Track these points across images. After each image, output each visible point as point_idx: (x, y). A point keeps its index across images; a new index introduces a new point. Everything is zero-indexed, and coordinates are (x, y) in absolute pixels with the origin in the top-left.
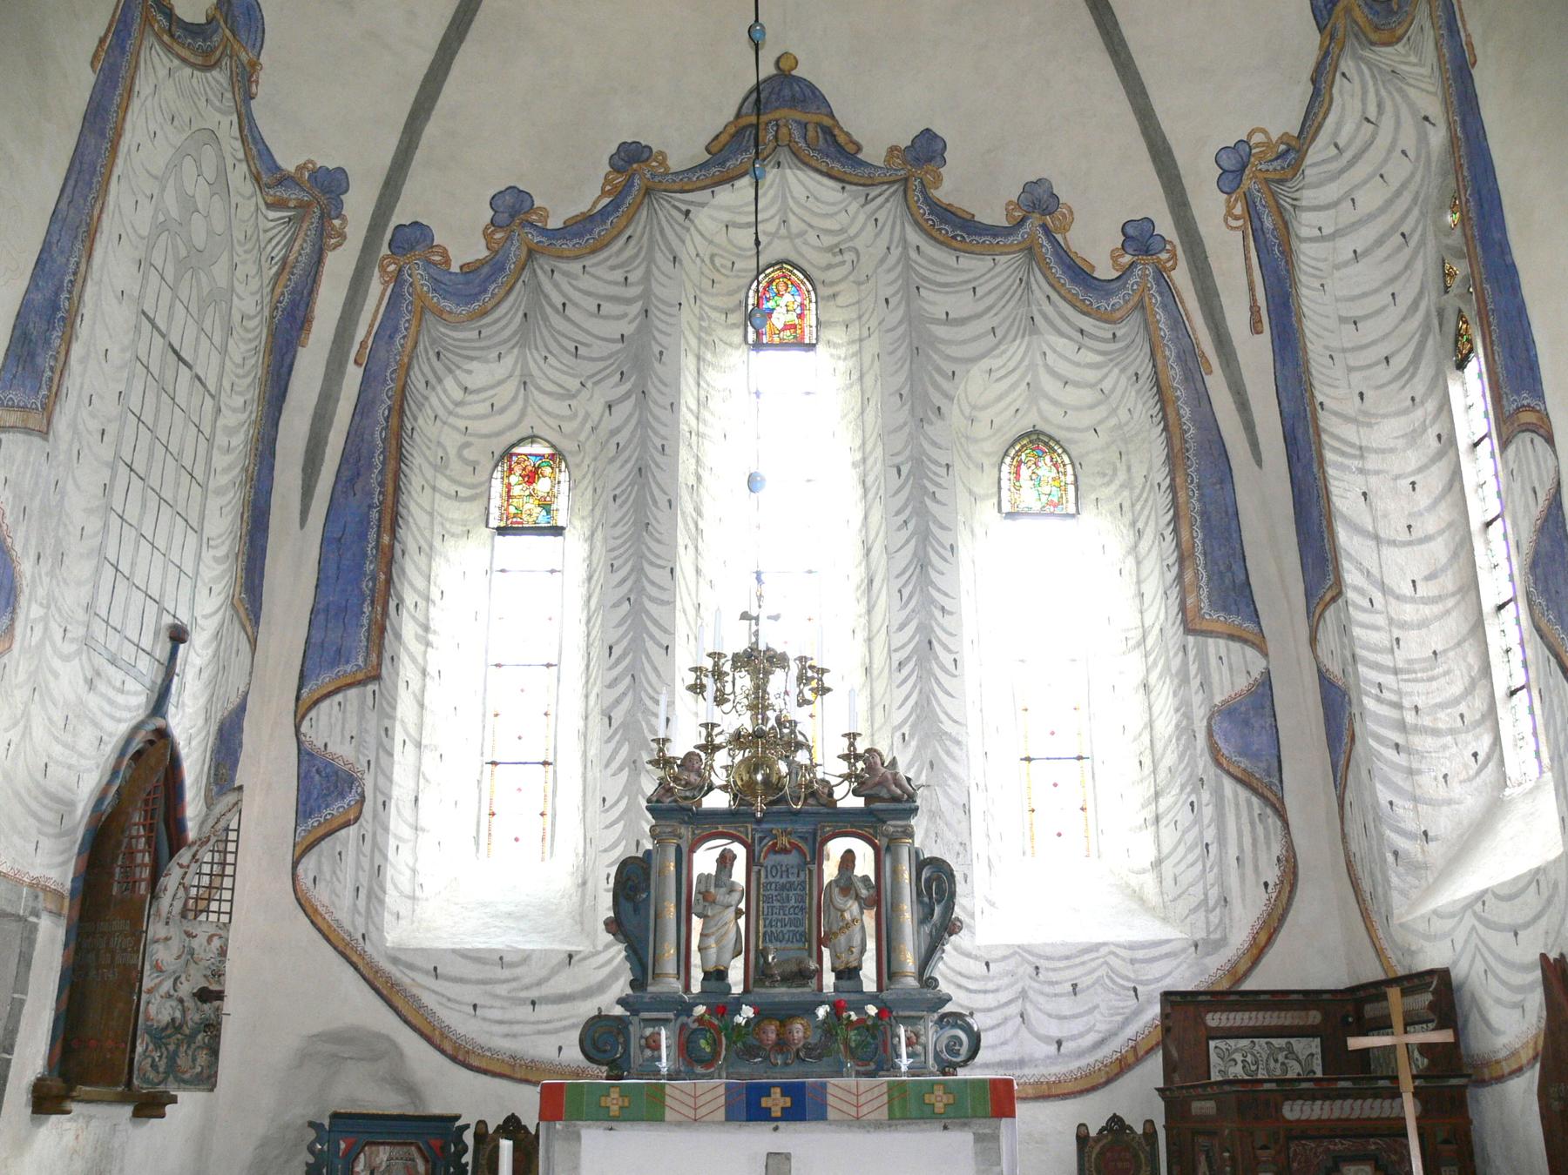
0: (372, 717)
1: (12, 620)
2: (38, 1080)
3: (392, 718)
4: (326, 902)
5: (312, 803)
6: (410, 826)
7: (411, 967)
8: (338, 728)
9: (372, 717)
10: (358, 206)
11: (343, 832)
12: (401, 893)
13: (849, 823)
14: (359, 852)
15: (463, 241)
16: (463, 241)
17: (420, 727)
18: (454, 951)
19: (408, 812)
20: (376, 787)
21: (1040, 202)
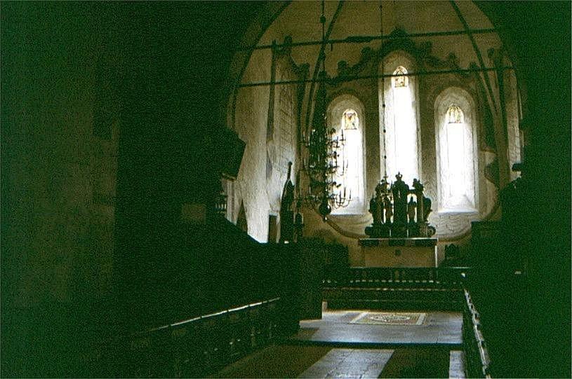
10: (312, 69)
13: (412, 192)
15: (332, 73)
16: (332, 73)
21: (452, 56)
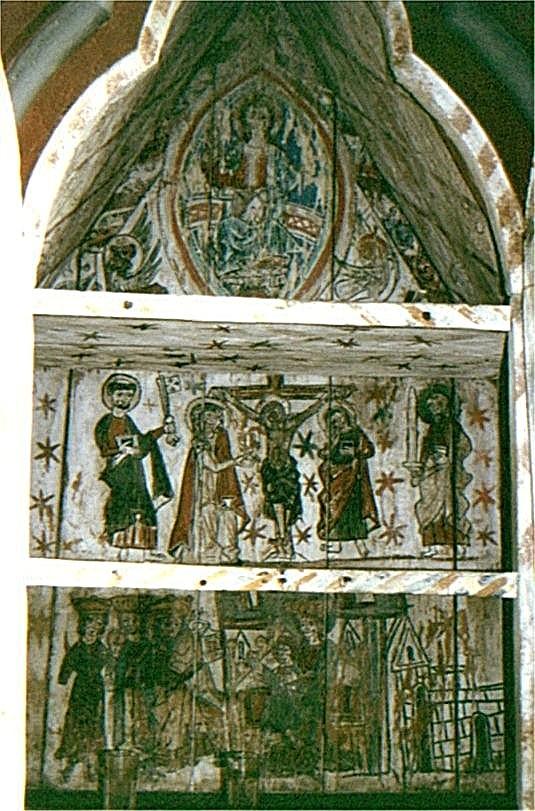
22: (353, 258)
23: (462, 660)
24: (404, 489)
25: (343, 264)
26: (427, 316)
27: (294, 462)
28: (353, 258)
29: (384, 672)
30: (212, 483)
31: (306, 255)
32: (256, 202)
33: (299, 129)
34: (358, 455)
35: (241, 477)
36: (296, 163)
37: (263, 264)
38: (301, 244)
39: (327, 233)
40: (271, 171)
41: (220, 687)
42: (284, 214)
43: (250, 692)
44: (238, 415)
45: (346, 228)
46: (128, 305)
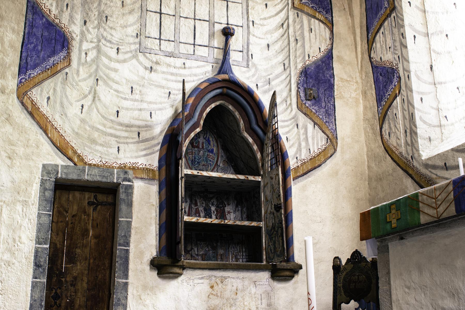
0: (395, 31)
1: (69, 53)
2: (154, 258)
3: (403, 26)
4: (395, 144)
5: (381, 93)
6: (430, 84)
7: (434, 167)
8: (384, 46)
9: (395, 31)
11: (395, 101)
12: (430, 125)
14: (403, 109)
17: (426, 24)
18: (453, 150)
19: (427, 76)
20: (404, 69)
22: (221, 165)
23: (244, 250)
24: (232, 214)
25: (219, 166)
26: (247, 178)
27: (210, 207)
28: (221, 165)
29: (229, 251)
30: (194, 211)
31: (212, 164)
32: (202, 152)
33: (210, 137)
34: (223, 206)
35: (200, 210)
36: (209, 144)
37: (203, 165)
38: (211, 161)
39: (216, 159)
40: (204, 145)
41: (196, 253)
42: (208, 155)
43: (203, 254)
44: (199, 197)
45: (220, 159)
46: (198, 173)
